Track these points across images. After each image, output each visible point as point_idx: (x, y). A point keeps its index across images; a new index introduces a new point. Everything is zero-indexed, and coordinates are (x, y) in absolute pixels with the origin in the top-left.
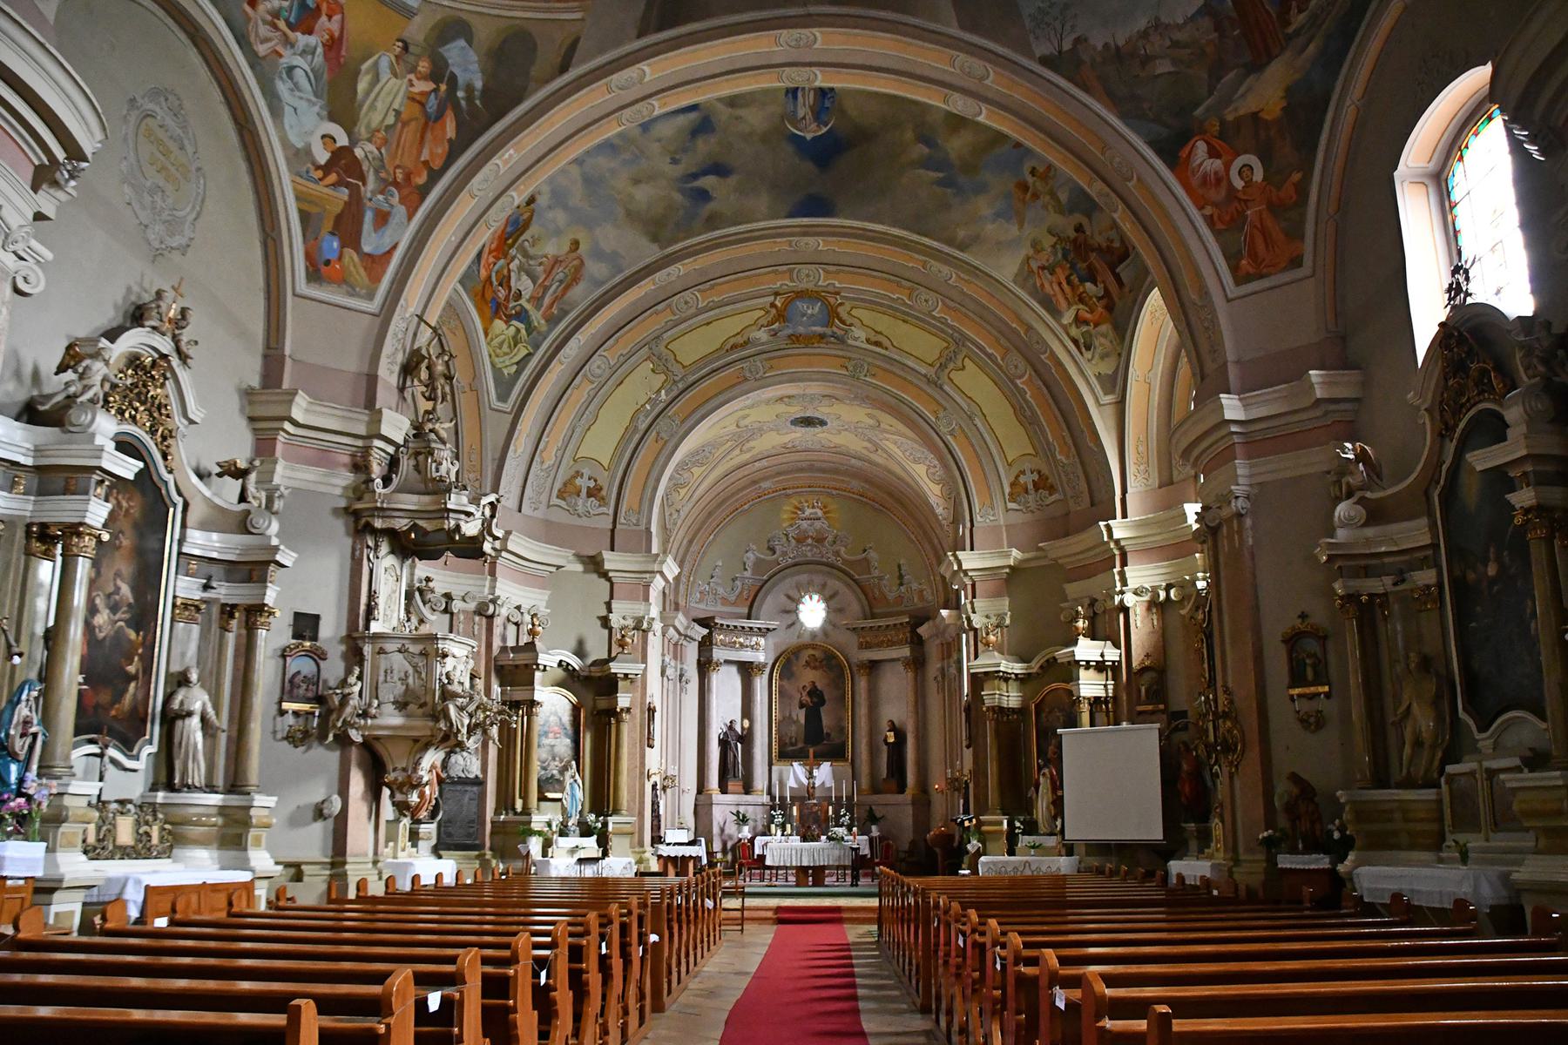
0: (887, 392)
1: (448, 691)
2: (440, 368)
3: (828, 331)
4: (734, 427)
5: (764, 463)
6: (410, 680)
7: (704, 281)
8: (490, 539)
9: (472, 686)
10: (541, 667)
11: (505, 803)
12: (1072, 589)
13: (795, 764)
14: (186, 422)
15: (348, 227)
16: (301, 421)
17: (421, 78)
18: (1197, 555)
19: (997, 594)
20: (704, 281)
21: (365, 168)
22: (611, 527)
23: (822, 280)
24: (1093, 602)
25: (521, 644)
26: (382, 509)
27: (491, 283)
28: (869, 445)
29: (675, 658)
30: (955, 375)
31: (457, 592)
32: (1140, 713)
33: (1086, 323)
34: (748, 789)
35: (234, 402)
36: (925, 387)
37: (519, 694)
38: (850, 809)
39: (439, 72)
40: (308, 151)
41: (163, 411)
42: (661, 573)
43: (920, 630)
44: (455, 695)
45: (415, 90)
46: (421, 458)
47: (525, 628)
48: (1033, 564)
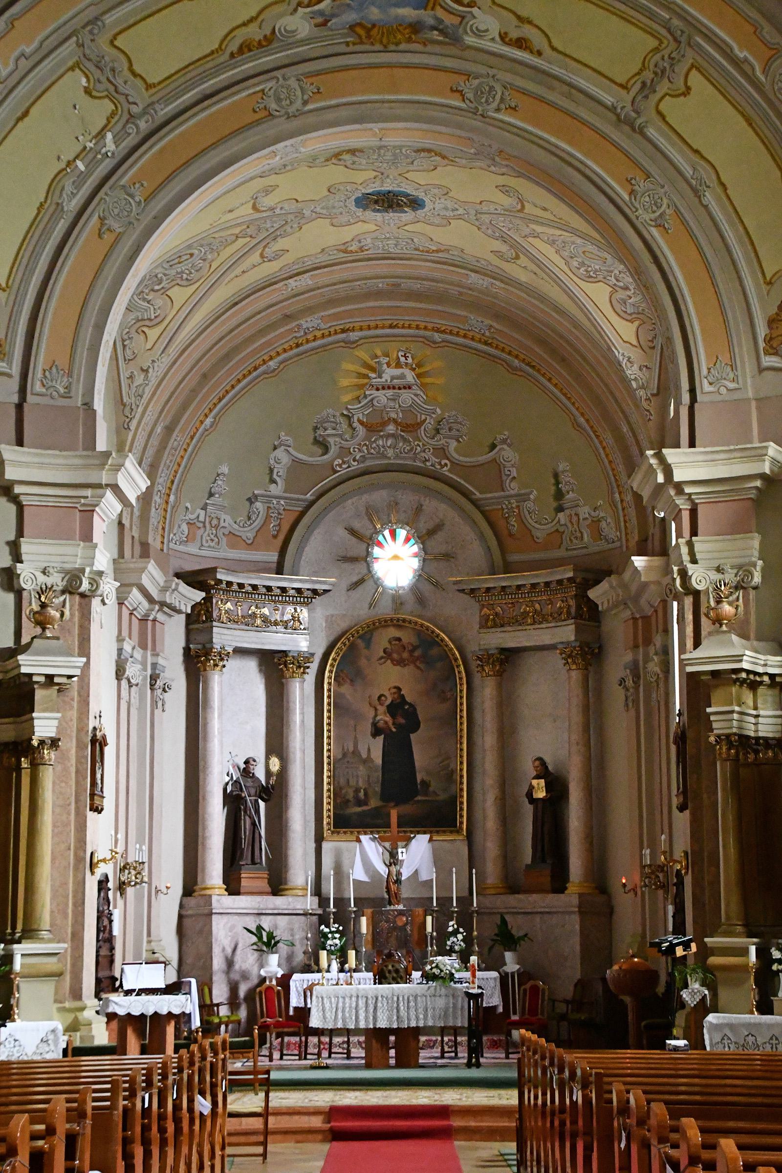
3: (426, 16)
4: (248, 209)
5: (306, 281)
13: (364, 838)
22: (15, 399)
28: (504, 248)
29: (143, 645)
36: (615, 135)
38: (465, 921)
42: (116, 489)
43: (592, 594)
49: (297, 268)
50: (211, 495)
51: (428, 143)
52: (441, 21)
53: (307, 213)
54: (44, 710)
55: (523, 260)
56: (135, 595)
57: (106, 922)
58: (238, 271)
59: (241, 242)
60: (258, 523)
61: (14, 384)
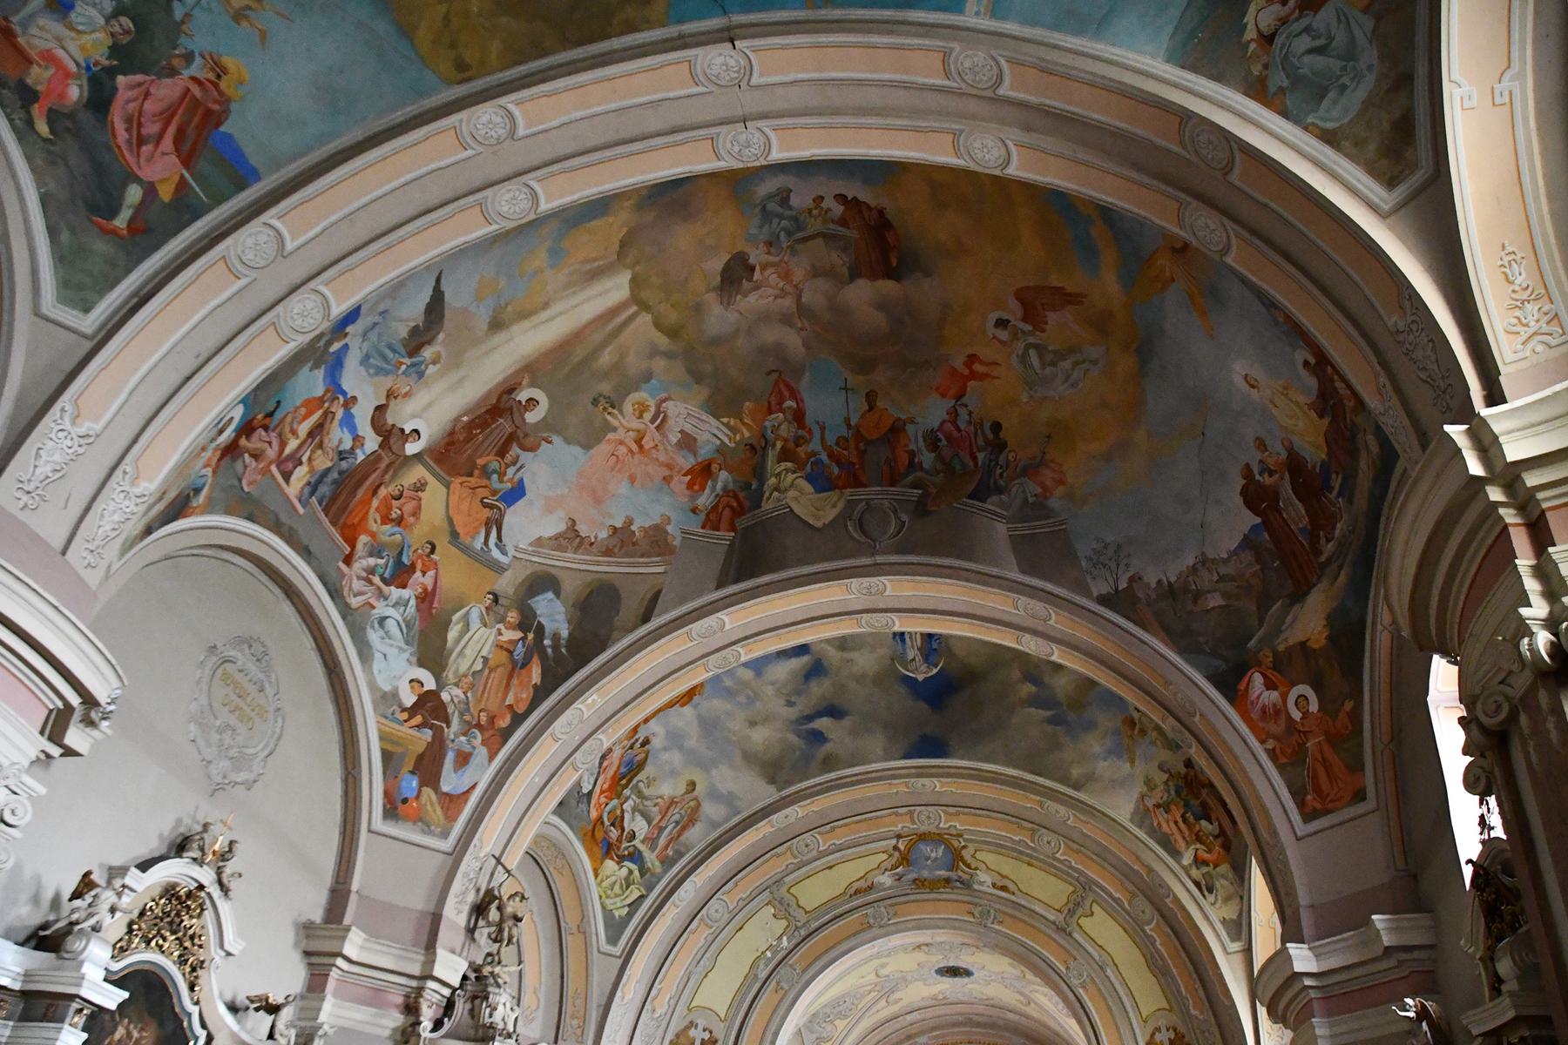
3: (953, 875)
4: (872, 977)
14: (223, 954)
15: (428, 767)
16: (354, 957)
17: (510, 627)
20: (824, 824)
21: (450, 710)
23: (929, 822)
27: (603, 823)
28: (1021, 998)
35: (289, 936)
39: (528, 622)
40: (394, 695)
41: (196, 941)
45: (503, 638)
46: (477, 1002)
49: (909, 1010)
51: (966, 941)
52: (960, 877)
53: (909, 978)
55: (1032, 1005)
58: (874, 1010)
59: (873, 994)
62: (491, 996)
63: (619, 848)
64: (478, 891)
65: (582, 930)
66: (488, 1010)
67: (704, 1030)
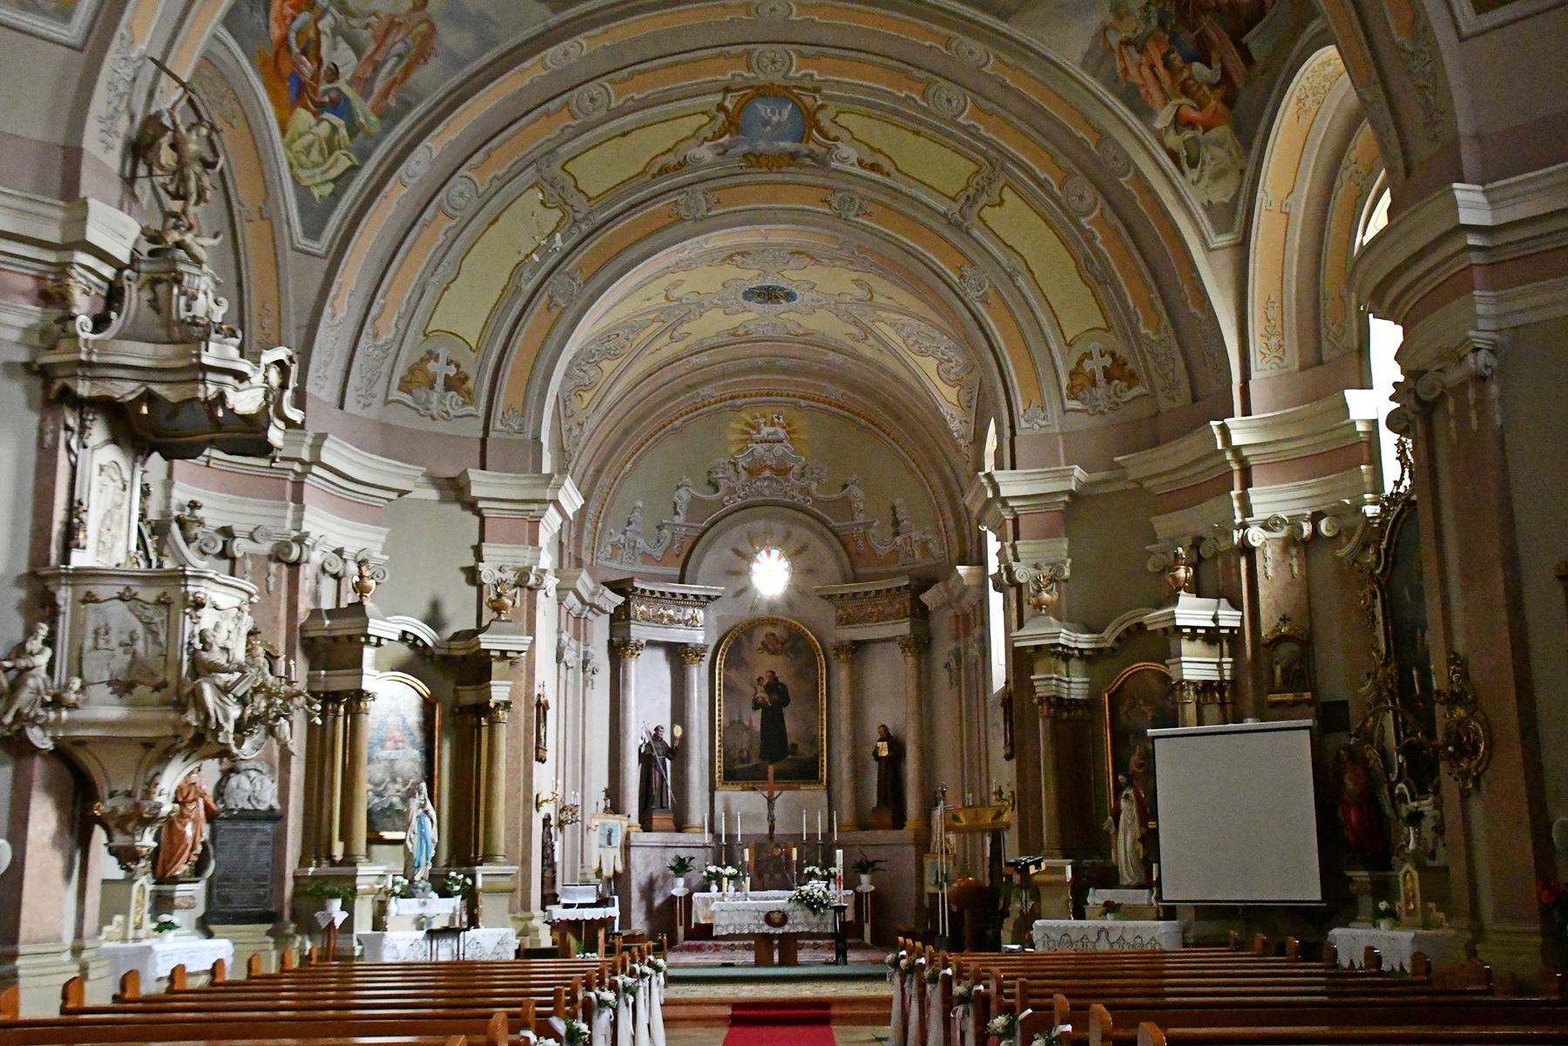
0: (886, 239)
1: (202, 662)
2: (194, 145)
3: (803, 148)
4: (661, 300)
5: (704, 358)
6: (140, 646)
7: (617, 67)
8: (281, 425)
9: (249, 651)
10: (374, 640)
11: (316, 846)
12: (1165, 525)
18: (1363, 467)
19: (1049, 533)
20: (617, 67)
22: (480, 434)
24: (1197, 543)
25: (343, 605)
26: (89, 365)
27: (289, 49)
29: (577, 638)
30: (987, 213)
31: (240, 525)
32: (1275, 704)
33: (1191, 124)
34: (680, 825)
36: (948, 233)
37: (339, 682)
42: (556, 503)
43: (925, 597)
44: (215, 668)
46: (162, 288)
47: (348, 584)
48: (1102, 490)
49: (697, 348)
50: (629, 523)
52: (812, 151)
53: (706, 303)
54: (500, 679)
55: (871, 341)
56: (571, 598)
57: (549, 851)
59: (656, 325)
60: (667, 543)
61: (480, 424)
62: (186, 278)
63: (315, 90)
64: (132, 117)
65: (268, 216)
66: (183, 300)
67: (448, 364)
